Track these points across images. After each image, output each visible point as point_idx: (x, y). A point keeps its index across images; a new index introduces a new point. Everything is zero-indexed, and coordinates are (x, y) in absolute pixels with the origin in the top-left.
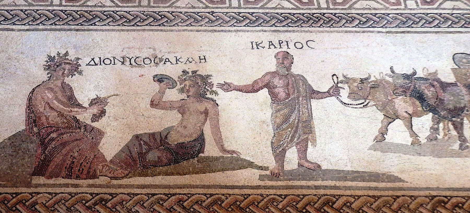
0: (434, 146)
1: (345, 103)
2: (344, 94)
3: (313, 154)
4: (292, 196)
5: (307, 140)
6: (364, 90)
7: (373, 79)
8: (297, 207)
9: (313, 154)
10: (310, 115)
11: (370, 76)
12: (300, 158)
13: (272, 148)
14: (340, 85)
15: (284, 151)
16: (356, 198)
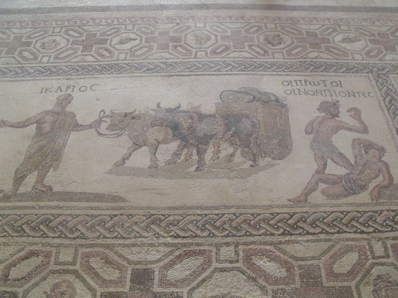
0: (172, 169)
1: (101, 134)
2: (104, 126)
3: (51, 178)
4: (13, 216)
5: (50, 167)
6: (122, 121)
7: (137, 112)
8: (13, 226)
9: (51, 178)
10: (64, 145)
11: (135, 111)
12: (37, 182)
13: (16, 173)
14: (104, 119)
15: (25, 176)
16: (56, 216)
